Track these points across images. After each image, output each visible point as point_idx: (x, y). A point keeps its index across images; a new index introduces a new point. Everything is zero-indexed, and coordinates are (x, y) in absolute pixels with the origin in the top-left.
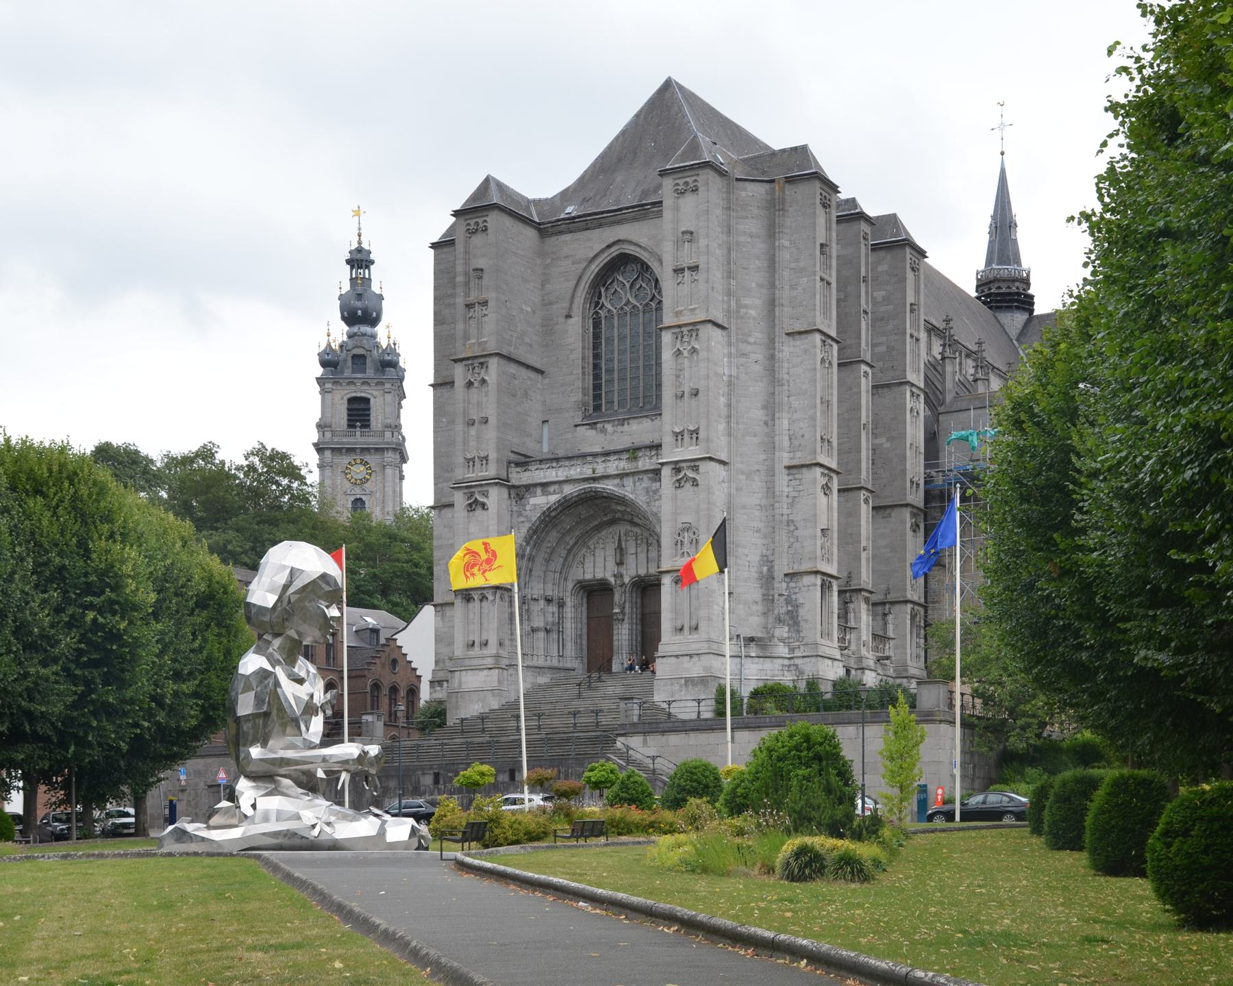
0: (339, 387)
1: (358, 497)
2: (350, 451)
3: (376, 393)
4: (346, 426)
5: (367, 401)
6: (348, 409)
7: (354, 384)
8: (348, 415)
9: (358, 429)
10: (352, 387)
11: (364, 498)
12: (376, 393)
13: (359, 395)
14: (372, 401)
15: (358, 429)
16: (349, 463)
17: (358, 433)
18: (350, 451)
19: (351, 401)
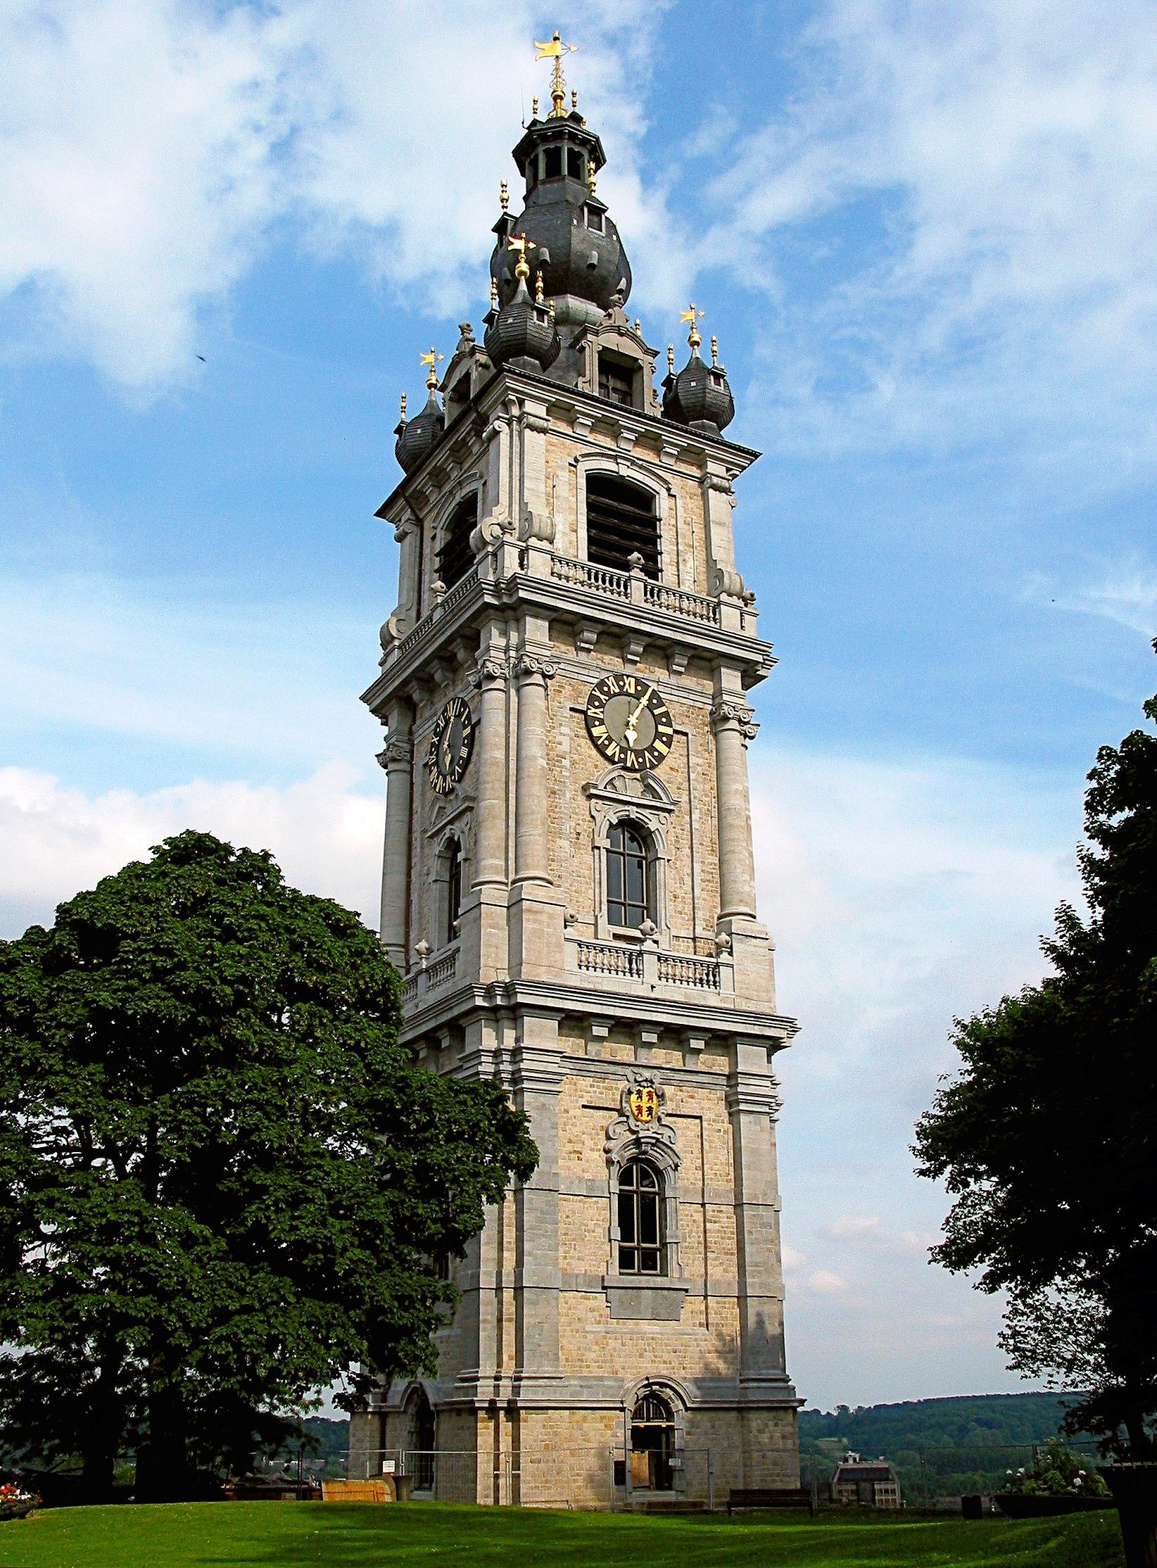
0: (563, 427)
1: (634, 813)
2: (615, 638)
3: (676, 482)
4: (583, 556)
5: (644, 499)
6: (591, 507)
7: (613, 430)
8: (591, 524)
9: (636, 573)
10: (607, 442)
11: (653, 823)
12: (676, 482)
13: (624, 471)
14: (663, 506)
15: (636, 573)
16: (601, 684)
17: (637, 588)
18: (615, 638)
19: (598, 484)
